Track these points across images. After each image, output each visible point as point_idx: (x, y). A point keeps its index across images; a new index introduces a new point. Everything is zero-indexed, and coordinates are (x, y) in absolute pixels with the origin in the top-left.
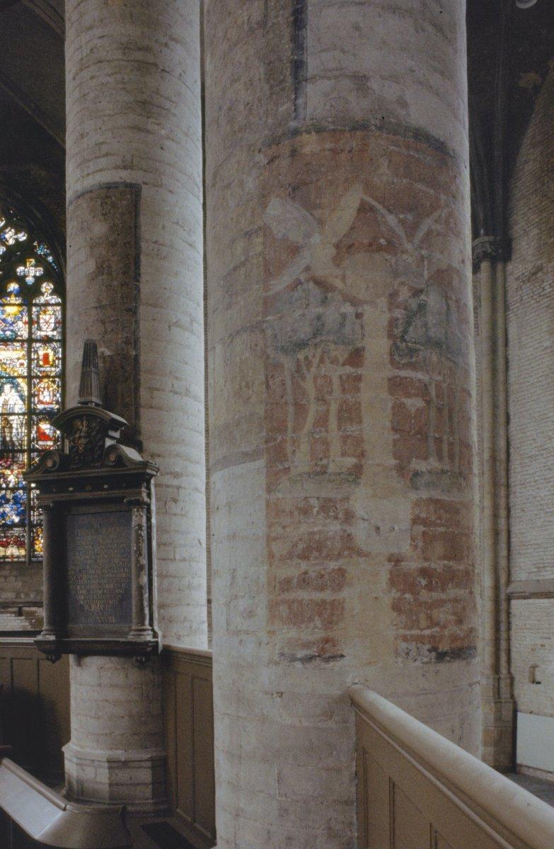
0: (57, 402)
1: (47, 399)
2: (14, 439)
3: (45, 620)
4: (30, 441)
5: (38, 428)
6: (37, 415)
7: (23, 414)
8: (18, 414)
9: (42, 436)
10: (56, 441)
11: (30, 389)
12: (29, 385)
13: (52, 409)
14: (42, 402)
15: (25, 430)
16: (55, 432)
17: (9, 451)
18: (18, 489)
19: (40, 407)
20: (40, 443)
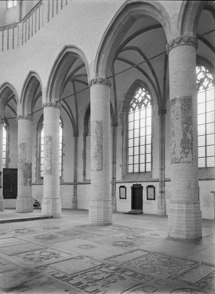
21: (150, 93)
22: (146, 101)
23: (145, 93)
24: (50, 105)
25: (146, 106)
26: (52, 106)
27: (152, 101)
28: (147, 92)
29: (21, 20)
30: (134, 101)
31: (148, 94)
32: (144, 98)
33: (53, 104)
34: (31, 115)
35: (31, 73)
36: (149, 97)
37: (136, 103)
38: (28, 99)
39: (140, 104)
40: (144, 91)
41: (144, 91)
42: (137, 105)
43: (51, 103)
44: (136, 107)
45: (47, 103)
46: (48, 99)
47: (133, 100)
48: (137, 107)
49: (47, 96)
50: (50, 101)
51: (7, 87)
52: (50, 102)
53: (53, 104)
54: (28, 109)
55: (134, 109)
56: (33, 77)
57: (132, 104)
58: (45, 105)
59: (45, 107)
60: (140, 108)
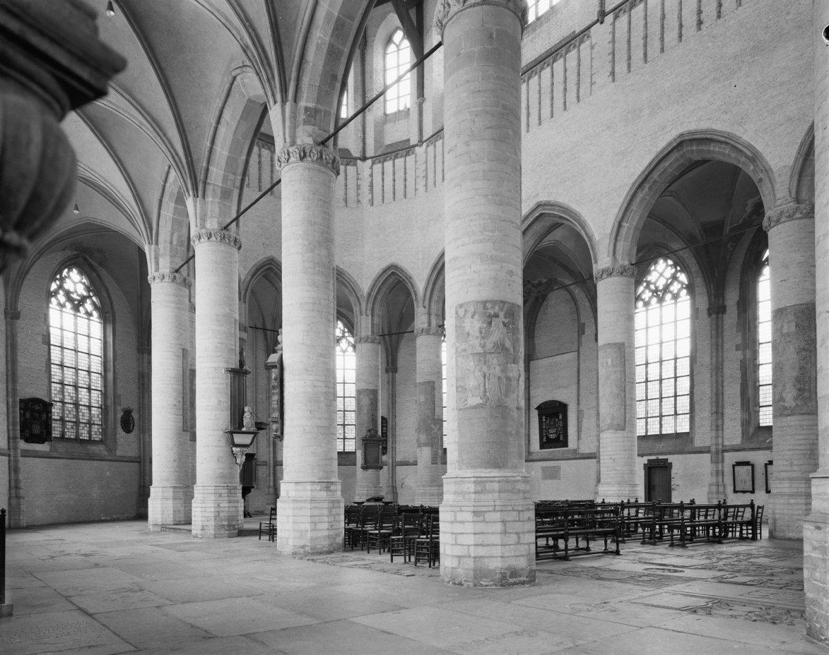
21: (685, 269)
22: (675, 287)
23: (674, 270)
25: (676, 297)
27: (690, 288)
28: (679, 268)
30: (648, 287)
31: (681, 271)
32: (669, 281)
36: (683, 277)
37: (650, 290)
39: (660, 294)
40: (671, 266)
41: (671, 266)
42: (653, 295)
44: (650, 298)
47: (645, 284)
48: (654, 300)
55: (647, 304)
57: (643, 292)
60: (661, 300)
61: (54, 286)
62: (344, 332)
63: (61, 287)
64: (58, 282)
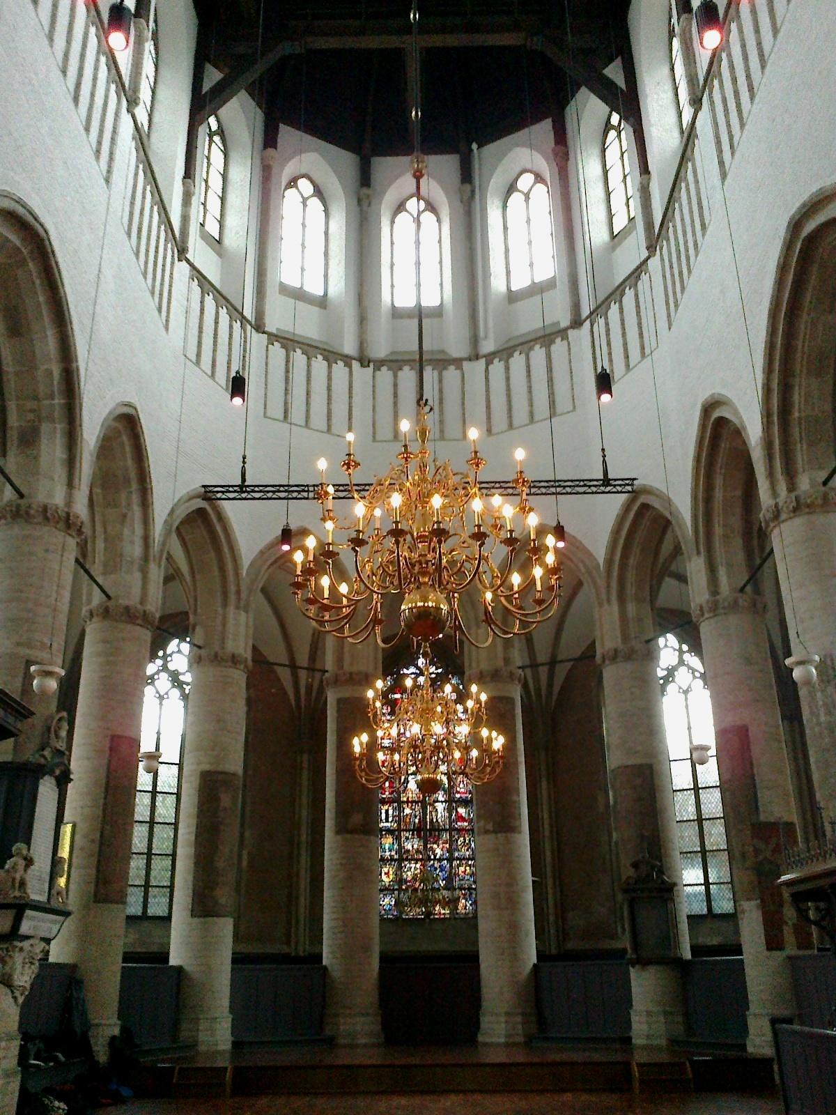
0: (470, 793)
1: (463, 790)
2: (439, 820)
3: (629, 949)
4: (450, 824)
5: (457, 811)
6: (456, 802)
7: (445, 801)
8: (442, 802)
9: (462, 819)
10: (470, 821)
11: (449, 783)
12: (449, 779)
13: (467, 797)
14: (458, 792)
15: (447, 814)
16: (469, 815)
17: (435, 830)
18: (444, 860)
19: (458, 796)
20: (459, 824)
24: (795, 510)
26: (807, 510)
29: (651, 248)
33: (809, 501)
34: (749, 589)
35: (708, 408)
38: (724, 526)
43: (797, 498)
45: (776, 505)
46: (782, 488)
49: (771, 475)
50: (792, 487)
51: (645, 507)
52: (793, 495)
53: (809, 501)
54: (729, 565)
56: (721, 421)
58: (769, 516)
59: (772, 525)
61: (151, 669)
62: (681, 652)
63: (165, 668)
64: (159, 662)
